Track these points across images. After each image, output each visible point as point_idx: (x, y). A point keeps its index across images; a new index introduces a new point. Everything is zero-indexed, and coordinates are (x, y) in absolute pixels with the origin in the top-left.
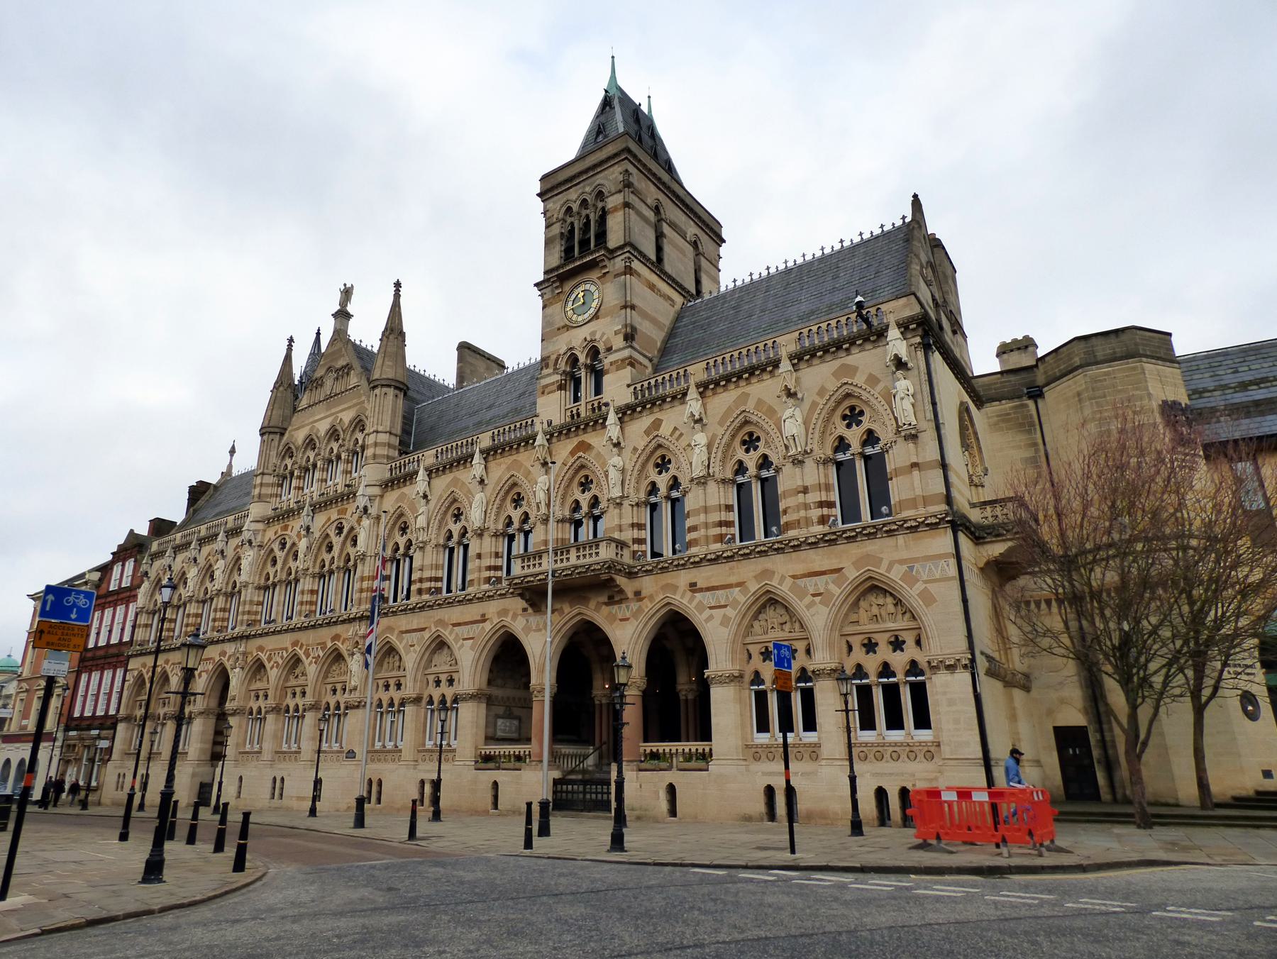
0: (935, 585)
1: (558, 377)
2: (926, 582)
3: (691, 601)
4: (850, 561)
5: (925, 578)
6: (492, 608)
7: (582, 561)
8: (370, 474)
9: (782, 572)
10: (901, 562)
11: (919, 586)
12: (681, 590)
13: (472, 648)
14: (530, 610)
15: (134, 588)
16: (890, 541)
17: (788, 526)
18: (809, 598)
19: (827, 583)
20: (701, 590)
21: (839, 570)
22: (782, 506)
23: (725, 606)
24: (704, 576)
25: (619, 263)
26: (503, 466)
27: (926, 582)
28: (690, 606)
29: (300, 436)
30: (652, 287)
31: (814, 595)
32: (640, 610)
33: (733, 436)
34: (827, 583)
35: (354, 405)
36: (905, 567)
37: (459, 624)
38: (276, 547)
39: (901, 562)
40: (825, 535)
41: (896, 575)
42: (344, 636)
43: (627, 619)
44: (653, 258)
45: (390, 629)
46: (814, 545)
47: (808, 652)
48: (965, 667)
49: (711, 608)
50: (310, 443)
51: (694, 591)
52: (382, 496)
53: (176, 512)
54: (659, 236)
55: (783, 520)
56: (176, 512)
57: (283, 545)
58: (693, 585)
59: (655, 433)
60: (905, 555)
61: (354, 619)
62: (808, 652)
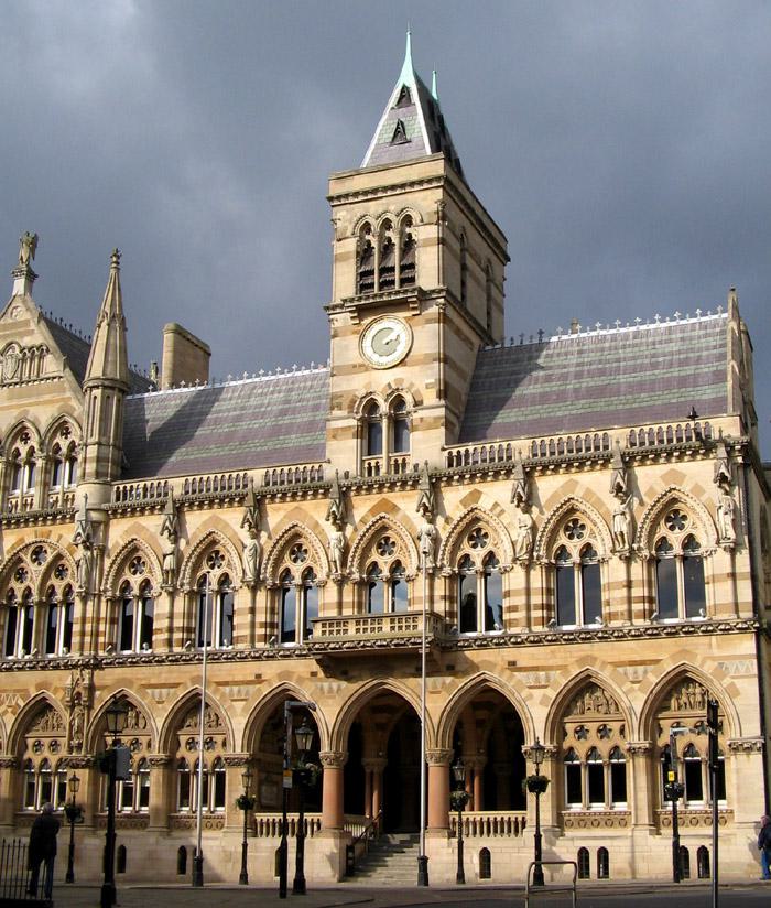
0: (741, 680)
2: (733, 677)
3: (512, 677)
4: (667, 655)
5: (732, 674)
6: (271, 670)
7: (396, 632)
9: (603, 659)
10: (713, 659)
11: (727, 681)
12: (498, 668)
13: (244, 709)
14: (321, 674)
16: (705, 640)
17: (611, 616)
18: (629, 685)
19: (645, 672)
20: (521, 669)
21: (657, 662)
22: (605, 596)
23: (546, 687)
24: (525, 656)
26: (282, 514)
27: (733, 677)
31: (633, 682)
32: (453, 684)
34: (645, 672)
35: (58, 401)
36: (716, 664)
37: (226, 684)
39: (713, 659)
40: (647, 629)
41: (707, 669)
42: (57, 684)
43: (439, 692)
46: (637, 637)
47: (622, 731)
48: (759, 750)
49: (530, 687)
51: (513, 671)
55: (605, 610)
58: (512, 664)
59: (474, 506)
60: (716, 652)
61: (75, 666)
62: (622, 731)
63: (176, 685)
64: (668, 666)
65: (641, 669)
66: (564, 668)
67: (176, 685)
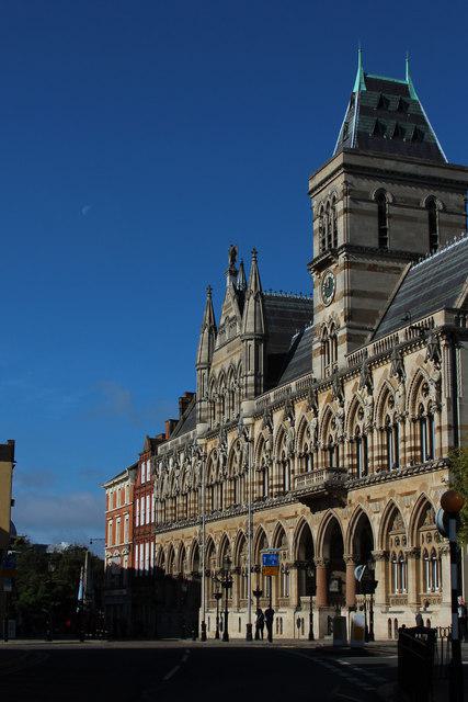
1: (319, 344)
8: (247, 406)
15: (151, 483)
25: (341, 259)
28: (368, 509)
29: (217, 371)
30: (373, 268)
33: (384, 400)
38: (212, 456)
44: (374, 243)
45: (262, 520)
50: (223, 377)
52: (253, 424)
53: (177, 416)
54: (382, 216)
56: (177, 416)
57: (215, 454)
63: (274, 521)
64: (418, 494)
65: (409, 497)
66: (384, 498)
67: (274, 521)
